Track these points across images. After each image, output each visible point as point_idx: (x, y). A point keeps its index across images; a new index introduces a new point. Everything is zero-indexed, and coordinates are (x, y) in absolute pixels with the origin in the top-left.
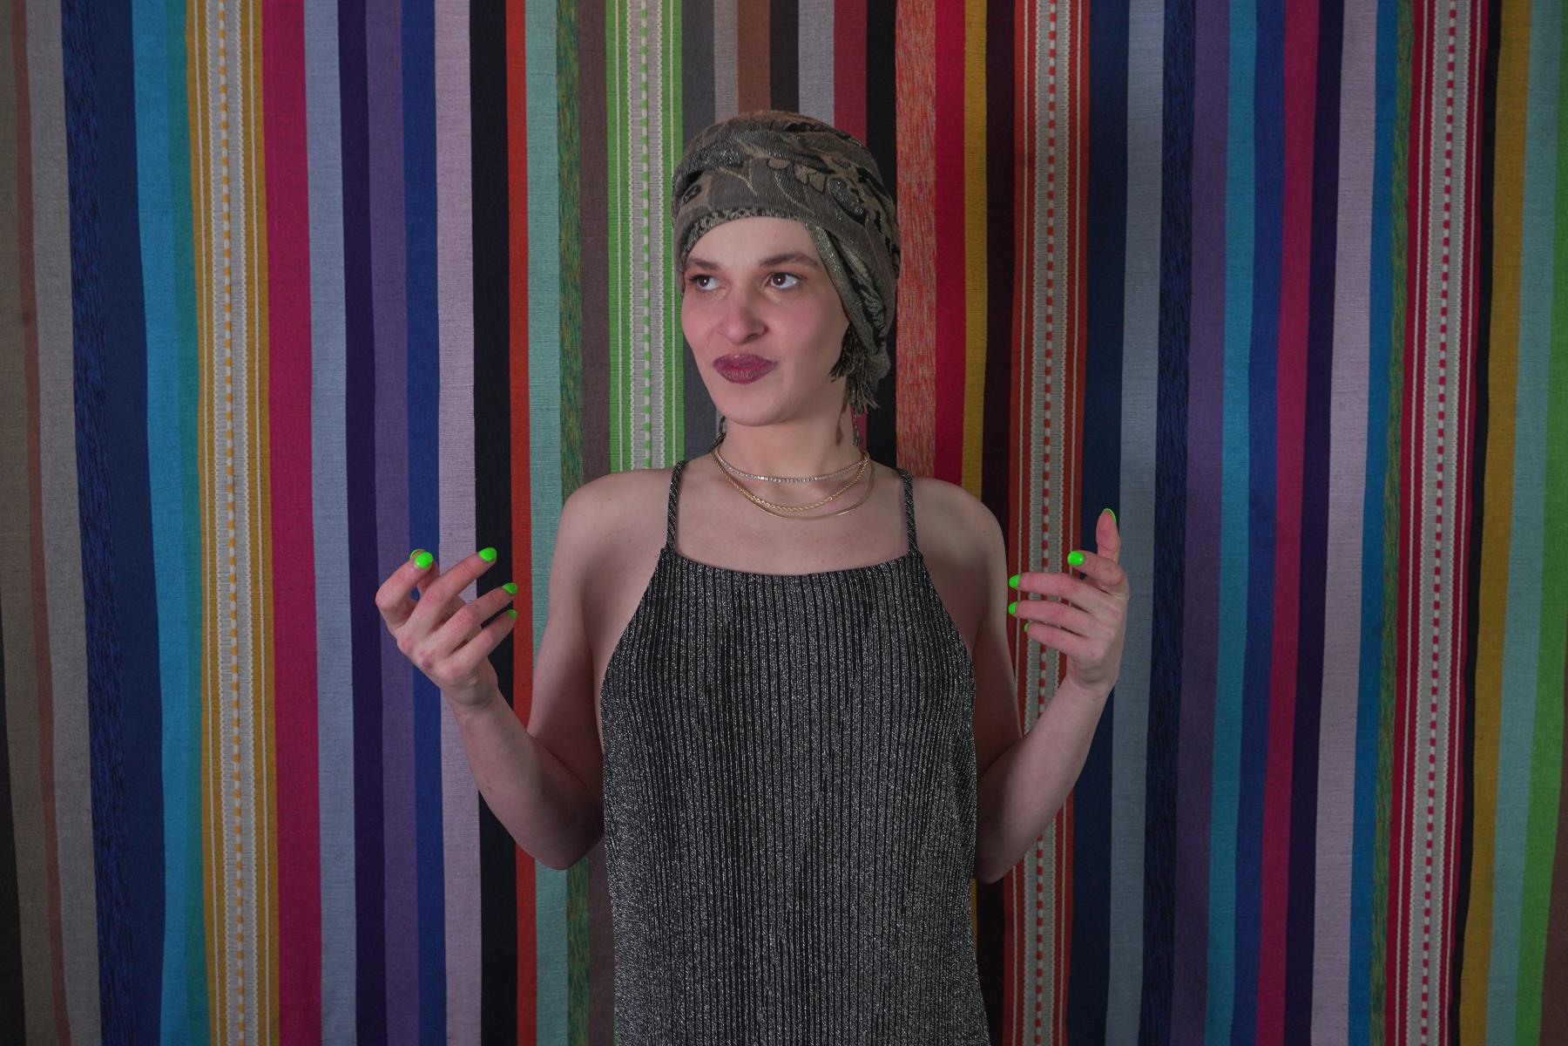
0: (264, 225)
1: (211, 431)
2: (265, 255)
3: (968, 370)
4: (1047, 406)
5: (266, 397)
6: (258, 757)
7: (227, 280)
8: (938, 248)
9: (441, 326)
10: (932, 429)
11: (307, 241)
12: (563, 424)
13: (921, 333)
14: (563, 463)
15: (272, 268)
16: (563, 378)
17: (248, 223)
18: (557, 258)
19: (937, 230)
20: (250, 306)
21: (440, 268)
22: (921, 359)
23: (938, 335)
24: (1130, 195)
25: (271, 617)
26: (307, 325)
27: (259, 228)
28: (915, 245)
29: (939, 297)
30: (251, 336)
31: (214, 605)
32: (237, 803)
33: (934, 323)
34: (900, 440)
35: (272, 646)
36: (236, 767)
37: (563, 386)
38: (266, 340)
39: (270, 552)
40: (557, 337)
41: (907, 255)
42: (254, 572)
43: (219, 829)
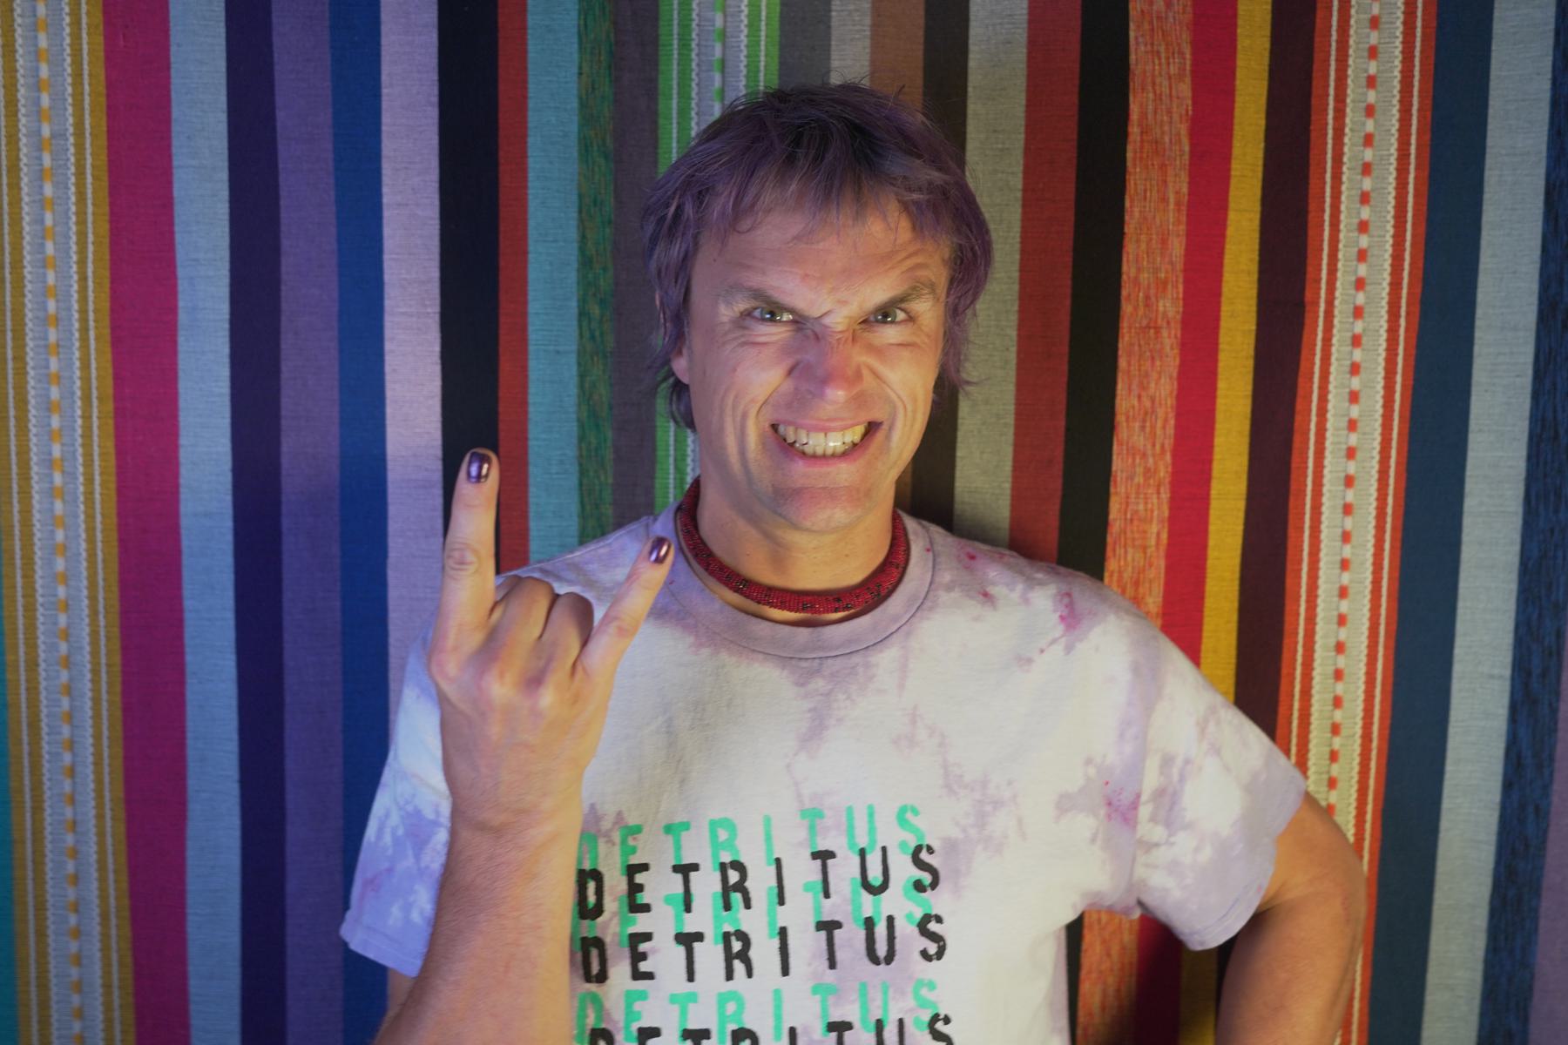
0: (100, 39)
1: (21, 372)
2: (102, 89)
3: (1225, 309)
4: (1355, 369)
5: (106, 322)
6: (102, 880)
7: (46, 131)
8: (1195, 102)
9: (387, 214)
10: (1171, 402)
11: (168, 67)
12: (582, 376)
13: (1164, 242)
14: (581, 438)
15: (112, 111)
16: (583, 302)
17: (76, 37)
18: (575, 104)
19: (1194, 73)
20: (80, 173)
21: (386, 119)
22: (1162, 285)
23: (1187, 250)
24: (1497, 28)
25: (117, 669)
26: (167, 204)
27: (91, 44)
28: (1158, 98)
29: (1192, 183)
30: (81, 222)
31: (32, 645)
32: (74, 947)
33: (1183, 227)
34: (1120, 418)
35: (119, 714)
36: (71, 893)
37: (583, 314)
38: (105, 227)
39: (115, 566)
40: (573, 234)
41: (1144, 115)
42: (93, 598)
43: (43, 986)
